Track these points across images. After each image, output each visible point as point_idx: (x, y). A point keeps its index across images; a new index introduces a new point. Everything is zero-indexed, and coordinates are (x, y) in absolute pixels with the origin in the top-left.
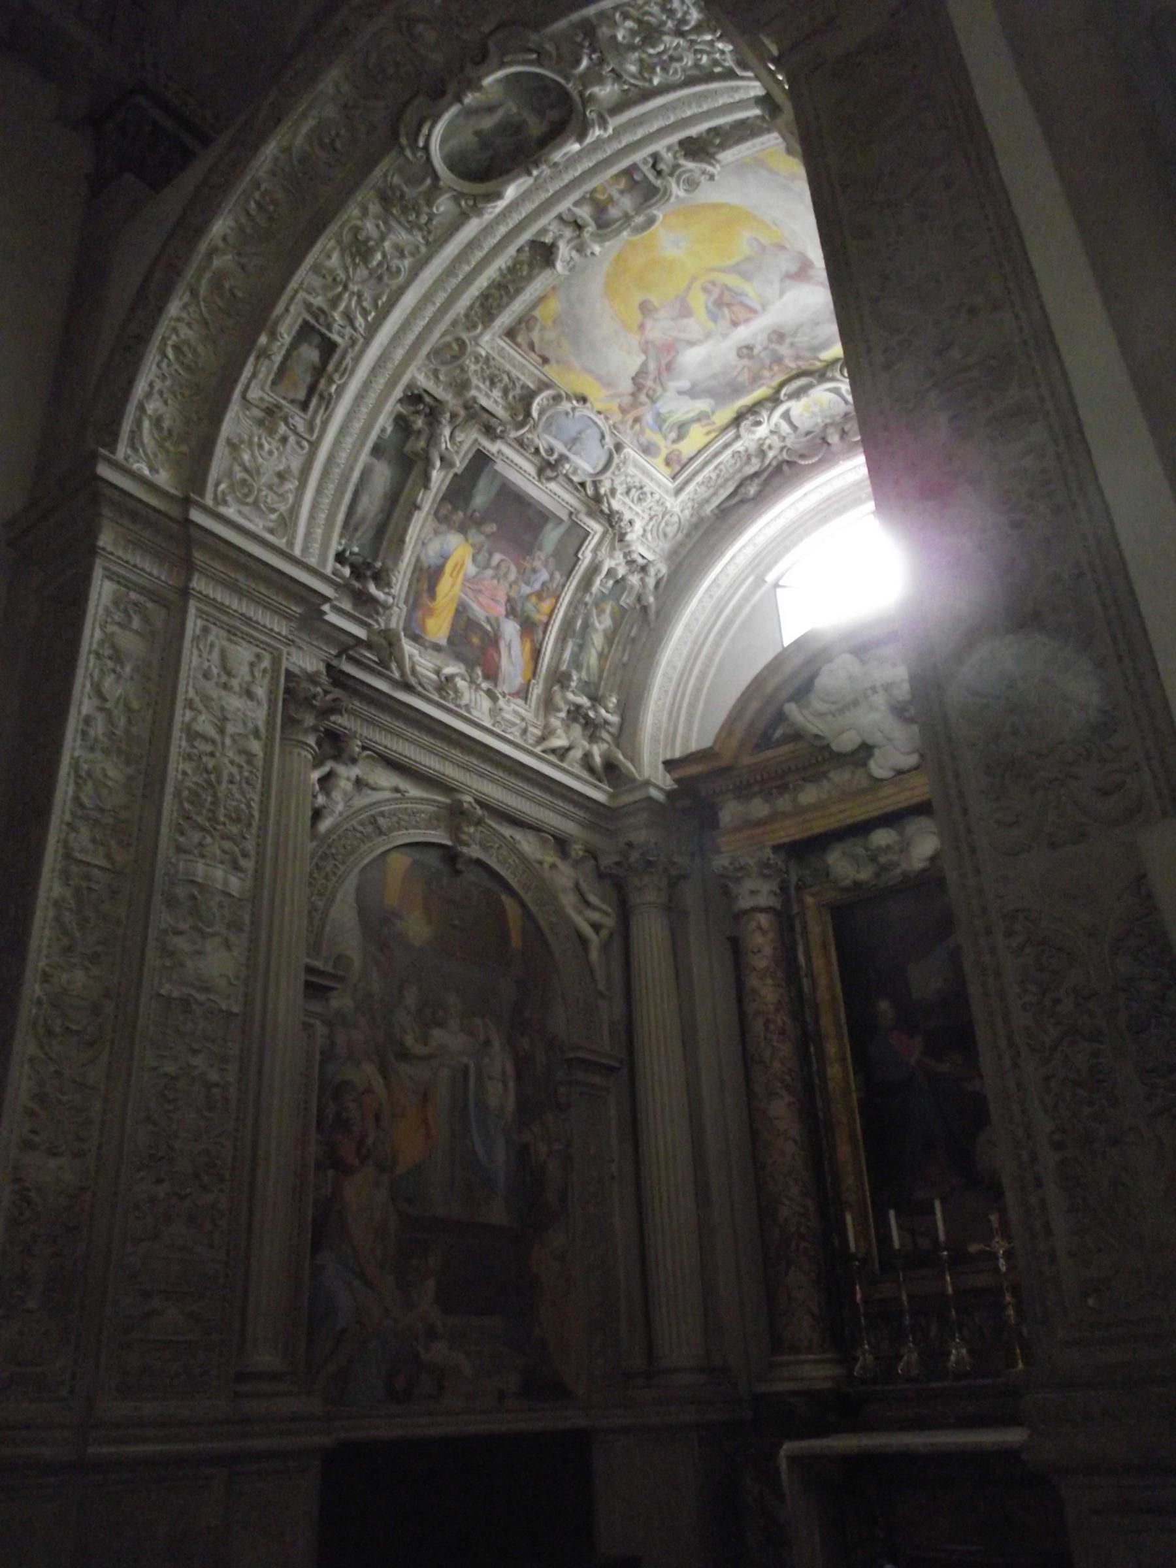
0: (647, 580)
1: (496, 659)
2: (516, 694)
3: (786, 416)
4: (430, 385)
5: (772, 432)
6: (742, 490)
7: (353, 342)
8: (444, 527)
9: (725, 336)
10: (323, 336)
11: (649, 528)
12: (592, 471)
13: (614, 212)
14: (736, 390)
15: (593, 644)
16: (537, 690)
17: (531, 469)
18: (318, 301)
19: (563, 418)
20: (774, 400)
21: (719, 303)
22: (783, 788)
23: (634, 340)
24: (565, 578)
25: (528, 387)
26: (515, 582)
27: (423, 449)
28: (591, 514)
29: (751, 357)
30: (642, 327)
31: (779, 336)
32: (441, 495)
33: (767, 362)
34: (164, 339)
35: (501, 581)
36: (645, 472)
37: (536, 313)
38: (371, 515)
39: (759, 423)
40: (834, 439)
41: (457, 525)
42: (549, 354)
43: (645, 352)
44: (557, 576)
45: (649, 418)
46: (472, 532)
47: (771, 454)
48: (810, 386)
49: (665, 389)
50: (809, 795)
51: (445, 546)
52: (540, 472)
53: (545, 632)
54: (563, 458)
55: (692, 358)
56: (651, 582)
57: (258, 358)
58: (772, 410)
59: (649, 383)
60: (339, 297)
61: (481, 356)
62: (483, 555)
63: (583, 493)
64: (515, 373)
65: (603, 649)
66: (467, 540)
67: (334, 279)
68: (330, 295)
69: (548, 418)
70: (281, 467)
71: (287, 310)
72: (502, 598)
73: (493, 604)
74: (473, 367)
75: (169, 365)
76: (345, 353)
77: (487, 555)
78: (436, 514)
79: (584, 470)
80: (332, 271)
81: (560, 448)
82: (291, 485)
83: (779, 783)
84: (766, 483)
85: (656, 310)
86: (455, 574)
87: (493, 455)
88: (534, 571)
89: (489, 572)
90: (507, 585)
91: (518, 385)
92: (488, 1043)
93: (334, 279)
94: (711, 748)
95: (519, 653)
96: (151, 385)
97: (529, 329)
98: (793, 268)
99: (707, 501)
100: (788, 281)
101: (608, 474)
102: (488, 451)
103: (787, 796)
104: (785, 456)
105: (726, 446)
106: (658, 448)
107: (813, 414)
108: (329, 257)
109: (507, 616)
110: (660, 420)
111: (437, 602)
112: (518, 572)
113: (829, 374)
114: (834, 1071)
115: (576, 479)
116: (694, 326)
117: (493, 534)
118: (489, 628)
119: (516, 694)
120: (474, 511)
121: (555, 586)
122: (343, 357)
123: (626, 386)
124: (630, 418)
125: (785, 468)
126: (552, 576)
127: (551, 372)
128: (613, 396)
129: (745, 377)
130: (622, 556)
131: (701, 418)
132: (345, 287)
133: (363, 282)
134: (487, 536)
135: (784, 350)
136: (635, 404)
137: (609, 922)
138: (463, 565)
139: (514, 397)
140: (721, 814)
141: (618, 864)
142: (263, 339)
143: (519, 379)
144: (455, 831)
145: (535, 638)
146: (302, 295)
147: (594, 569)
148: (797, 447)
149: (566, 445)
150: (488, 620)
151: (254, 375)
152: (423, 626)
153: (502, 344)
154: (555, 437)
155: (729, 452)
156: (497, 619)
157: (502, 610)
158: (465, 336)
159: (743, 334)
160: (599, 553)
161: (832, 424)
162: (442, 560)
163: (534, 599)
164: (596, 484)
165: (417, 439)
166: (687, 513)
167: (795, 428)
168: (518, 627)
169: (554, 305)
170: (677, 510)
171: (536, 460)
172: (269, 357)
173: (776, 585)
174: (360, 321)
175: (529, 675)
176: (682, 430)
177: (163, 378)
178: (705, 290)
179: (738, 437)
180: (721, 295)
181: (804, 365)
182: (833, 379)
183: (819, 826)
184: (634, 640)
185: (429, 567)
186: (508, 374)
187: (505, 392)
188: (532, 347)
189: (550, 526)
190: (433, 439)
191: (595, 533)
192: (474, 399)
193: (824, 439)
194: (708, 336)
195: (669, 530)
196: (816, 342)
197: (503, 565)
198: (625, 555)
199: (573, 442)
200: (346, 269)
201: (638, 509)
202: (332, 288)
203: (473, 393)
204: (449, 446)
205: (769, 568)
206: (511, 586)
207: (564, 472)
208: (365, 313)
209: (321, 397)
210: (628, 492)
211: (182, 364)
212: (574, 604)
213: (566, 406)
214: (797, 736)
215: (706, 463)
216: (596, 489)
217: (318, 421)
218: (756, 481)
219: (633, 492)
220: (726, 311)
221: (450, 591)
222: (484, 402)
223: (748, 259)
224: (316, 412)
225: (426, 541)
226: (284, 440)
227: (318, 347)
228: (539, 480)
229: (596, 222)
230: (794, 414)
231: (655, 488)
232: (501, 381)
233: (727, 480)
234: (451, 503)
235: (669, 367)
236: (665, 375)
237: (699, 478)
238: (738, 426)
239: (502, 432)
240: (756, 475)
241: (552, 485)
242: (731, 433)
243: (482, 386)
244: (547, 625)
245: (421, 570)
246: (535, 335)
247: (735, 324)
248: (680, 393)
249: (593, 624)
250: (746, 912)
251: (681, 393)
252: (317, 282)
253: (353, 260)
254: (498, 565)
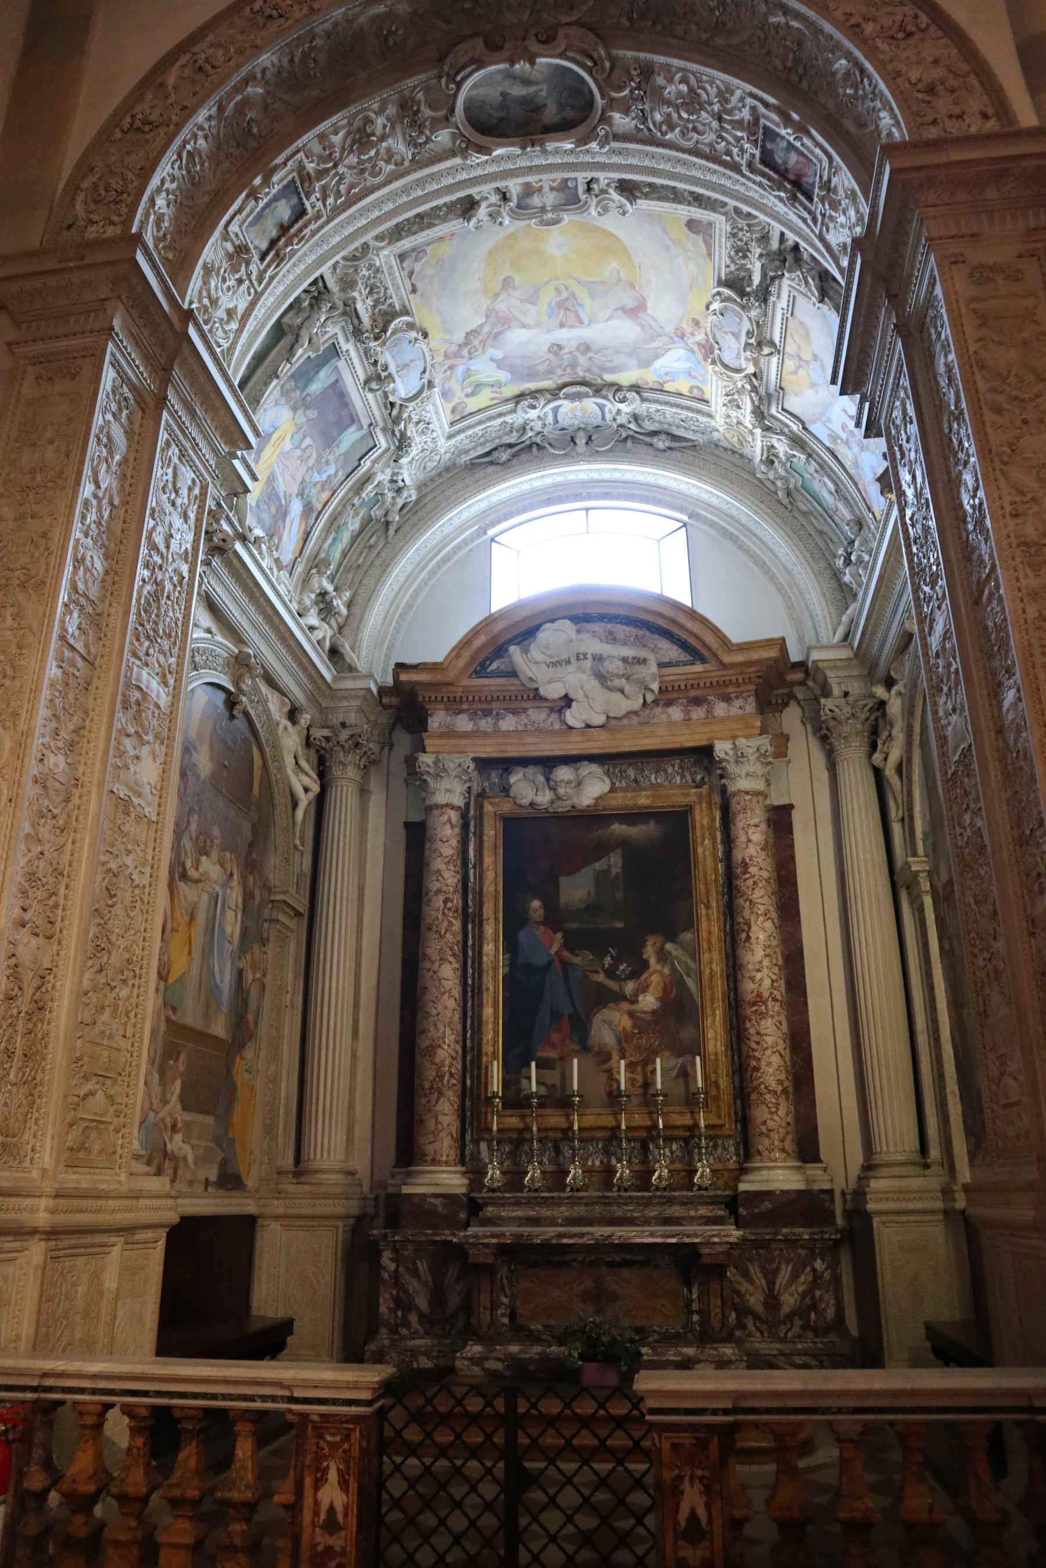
3: (555, 411)
5: (539, 417)
6: (496, 454)
7: (318, 216)
8: (283, 401)
9: (549, 330)
10: (301, 199)
13: (536, 201)
14: (531, 376)
16: (299, 569)
17: (362, 376)
18: (310, 167)
20: (555, 393)
21: (560, 305)
22: (487, 713)
23: (485, 304)
28: (384, 430)
29: (556, 354)
30: (497, 295)
31: (586, 348)
33: (566, 363)
34: (185, 142)
36: (437, 413)
37: (429, 249)
39: (534, 407)
40: (581, 440)
42: (418, 286)
43: (487, 317)
45: (460, 370)
47: (530, 434)
48: (587, 396)
49: (483, 352)
50: (508, 723)
52: (367, 382)
55: (516, 337)
57: (247, 196)
58: (549, 401)
59: (476, 342)
60: (327, 171)
64: (391, 291)
67: (331, 154)
68: (322, 166)
70: (231, 306)
71: (285, 164)
72: (299, 480)
74: (365, 272)
75: (180, 168)
76: (309, 222)
80: (332, 146)
81: (392, 369)
82: (234, 326)
83: (484, 706)
84: (515, 456)
85: (514, 288)
89: (298, 452)
91: (389, 301)
92: (231, 875)
93: (331, 154)
94: (442, 663)
96: (163, 182)
97: (417, 260)
98: (630, 304)
99: (466, 452)
100: (620, 312)
101: (413, 404)
103: (489, 719)
104: (538, 440)
105: (501, 415)
106: (453, 395)
107: (575, 417)
108: (336, 134)
110: (468, 374)
113: (604, 392)
114: (488, 948)
116: (532, 313)
122: (305, 226)
123: (459, 337)
124: (448, 363)
125: (535, 448)
127: (414, 302)
128: (445, 341)
129: (542, 368)
131: (496, 385)
132: (335, 166)
133: (351, 167)
135: (583, 361)
136: (457, 355)
137: (316, 788)
140: (430, 720)
141: (327, 739)
142: (258, 181)
144: (237, 681)
146: (301, 154)
147: (368, 478)
148: (551, 436)
151: (239, 211)
153: (394, 263)
155: (500, 420)
157: (295, 489)
159: (562, 335)
161: (584, 429)
166: (448, 456)
167: (556, 421)
169: (445, 250)
170: (443, 451)
171: (371, 370)
172: (257, 199)
173: (493, 540)
174: (330, 200)
176: (478, 387)
177: (173, 179)
178: (557, 290)
179: (513, 411)
180: (567, 299)
181: (588, 377)
182: (605, 398)
183: (513, 751)
184: (371, 546)
186: (386, 289)
187: (377, 302)
188: (411, 274)
192: (354, 299)
193: (573, 440)
194: (538, 325)
196: (608, 365)
198: (394, 474)
200: (343, 149)
202: (325, 162)
203: (355, 294)
205: (493, 524)
208: (338, 195)
209: (277, 255)
210: (418, 423)
211: (189, 172)
213: (413, 334)
214: (513, 674)
215: (479, 423)
216: (400, 412)
217: (268, 275)
218: (510, 451)
220: (562, 313)
222: (359, 306)
223: (604, 283)
224: (268, 266)
226: (240, 282)
227: (293, 208)
229: (519, 200)
230: (561, 410)
233: (486, 442)
235: (496, 336)
236: (490, 342)
237: (470, 432)
238: (517, 403)
240: (510, 446)
241: (370, 396)
242: (510, 406)
246: (418, 267)
247: (562, 325)
248: (492, 359)
250: (437, 806)
251: (492, 359)
252: (316, 148)
253: (352, 146)
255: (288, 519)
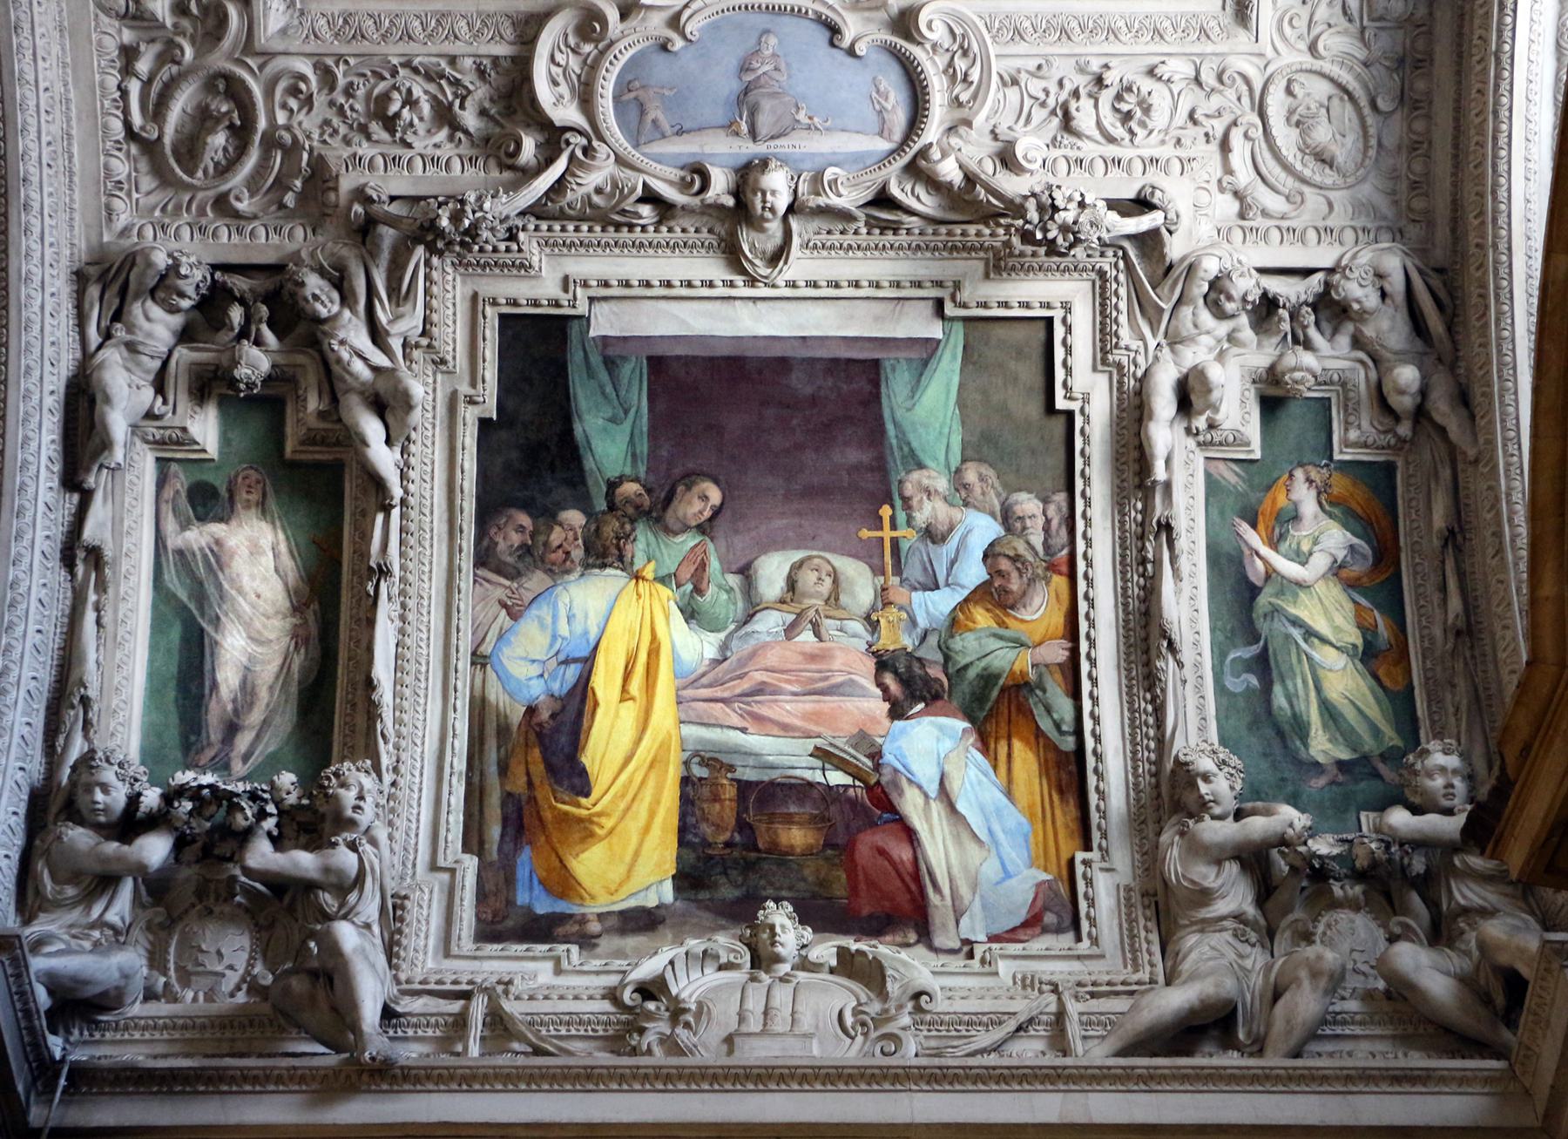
0: (1369, 331)
1: (903, 853)
2: (1033, 923)
4: (228, 244)
8: (535, 581)
11: (1244, 175)
12: (885, 146)
15: (1309, 633)
17: (711, 268)
19: (661, 69)
24: (1061, 497)
25: (495, 60)
26: (883, 598)
27: (322, 415)
28: (999, 264)
32: (469, 506)
35: (829, 625)
38: (268, 672)
41: (578, 553)
44: (1028, 504)
46: (642, 542)
51: (563, 629)
52: (732, 255)
53: (1076, 694)
54: (747, 176)
56: (1389, 328)
61: (303, 78)
62: (721, 593)
63: (913, 221)
64: (425, 53)
65: (1367, 630)
66: (637, 577)
69: (617, 99)
73: (830, 702)
74: (308, 123)
77: (734, 580)
78: (485, 558)
79: (857, 158)
86: (635, 686)
87: (557, 304)
88: (933, 535)
89: (770, 623)
90: (857, 627)
95: (993, 794)
102: (536, 304)
109: (897, 712)
111: (595, 794)
112: (878, 570)
115: (848, 198)
117: (717, 512)
118: (837, 778)
119: (1033, 923)
120: (613, 485)
121: (1037, 539)
126: (1007, 517)
130: (1206, 317)
134: (701, 529)
138: (654, 652)
139: (483, 113)
143: (452, 60)
145: (1045, 724)
149: (730, 128)
150: (824, 756)
152: (563, 883)
154: (680, 133)
156: (862, 739)
158: (219, 60)
160: (1118, 356)
162: (572, 672)
163: (982, 618)
164: (917, 171)
165: (301, 401)
168: (961, 725)
170: (1295, 56)
175: (1068, 845)
185: (531, 711)
187: (445, 116)
189: (896, 387)
190: (331, 377)
191: (1067, 307)
195: (1322, 134)
197: (808, 578)
199: (746, 102)
201: (1148, 146)
203: (347, 183)
204: (380, 359)
206: (873, 626)
207: (782, 203)
212: (1132, 554)
216: (935, 185)
219: (1084, 118)
221: (638, 741)
225: (486, 649)
228: (752, 281)
231: (1148, 48)
232: (410, 101)
234: (527, 506)
239: (456, 218)
241: (799, 266)
243: (365, 150)
244: (1071, 672)
245: (503, 731)
249: (1271, 573)
254: (792, 584)
255: (911, 805)
